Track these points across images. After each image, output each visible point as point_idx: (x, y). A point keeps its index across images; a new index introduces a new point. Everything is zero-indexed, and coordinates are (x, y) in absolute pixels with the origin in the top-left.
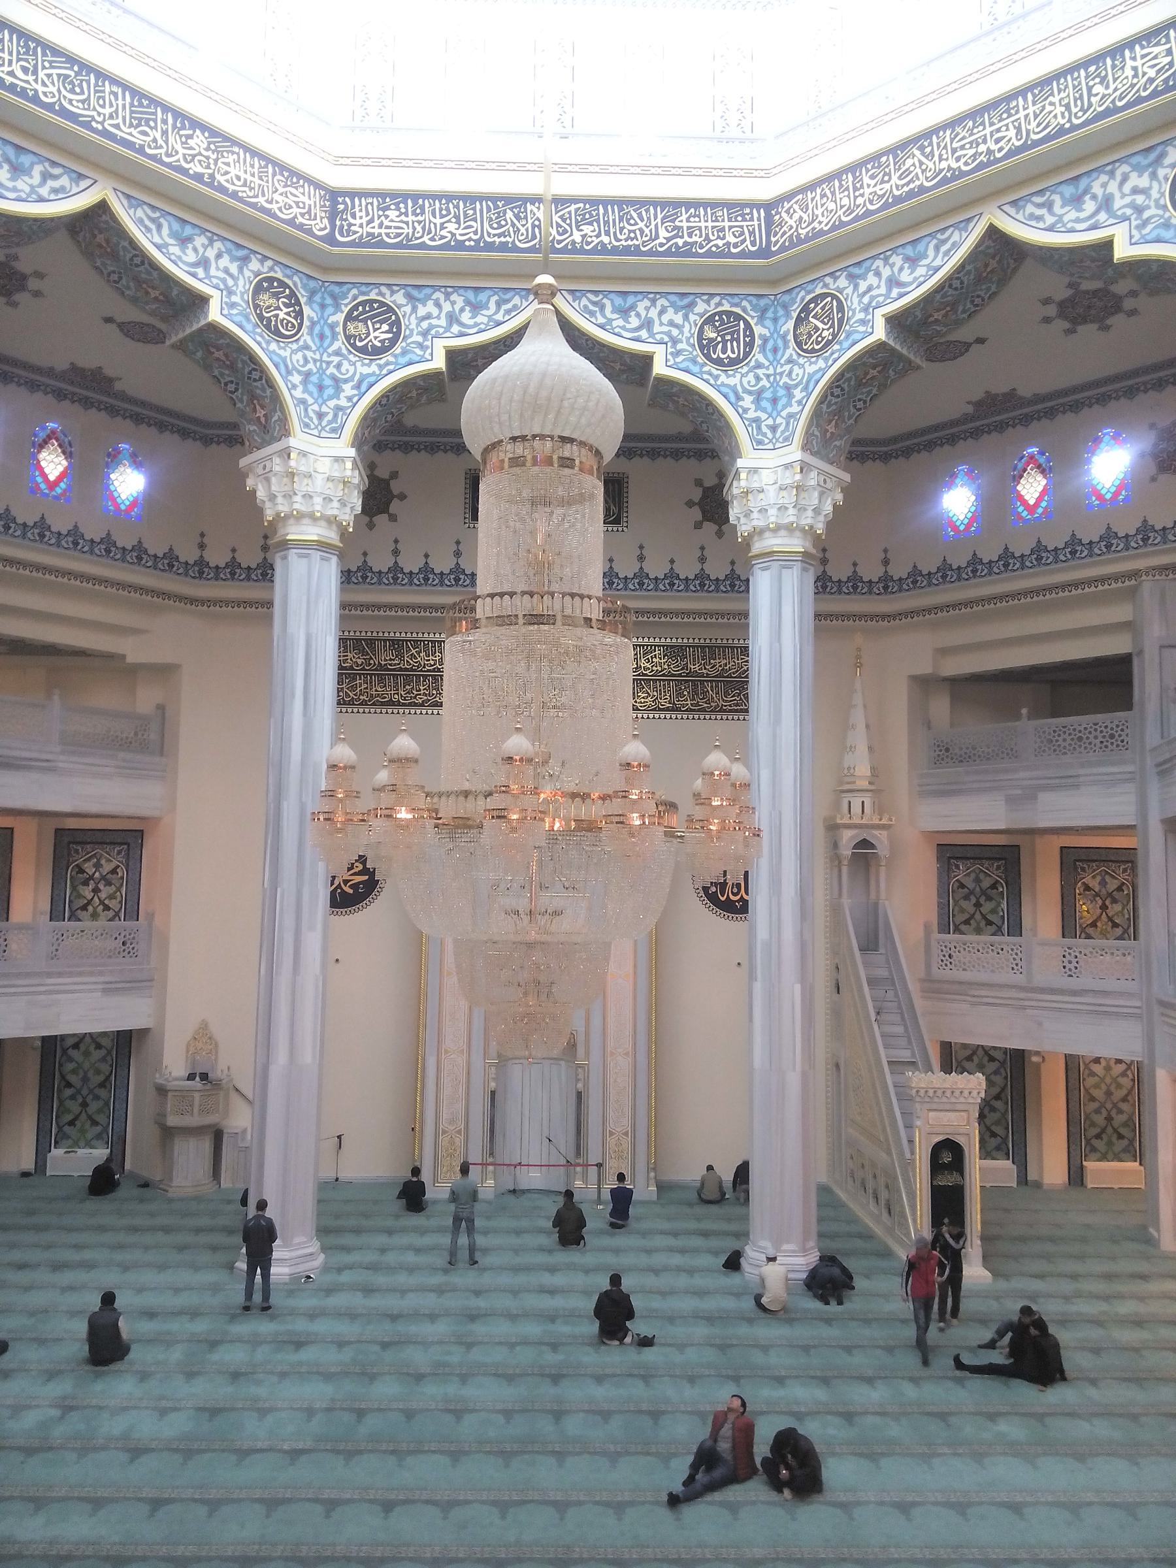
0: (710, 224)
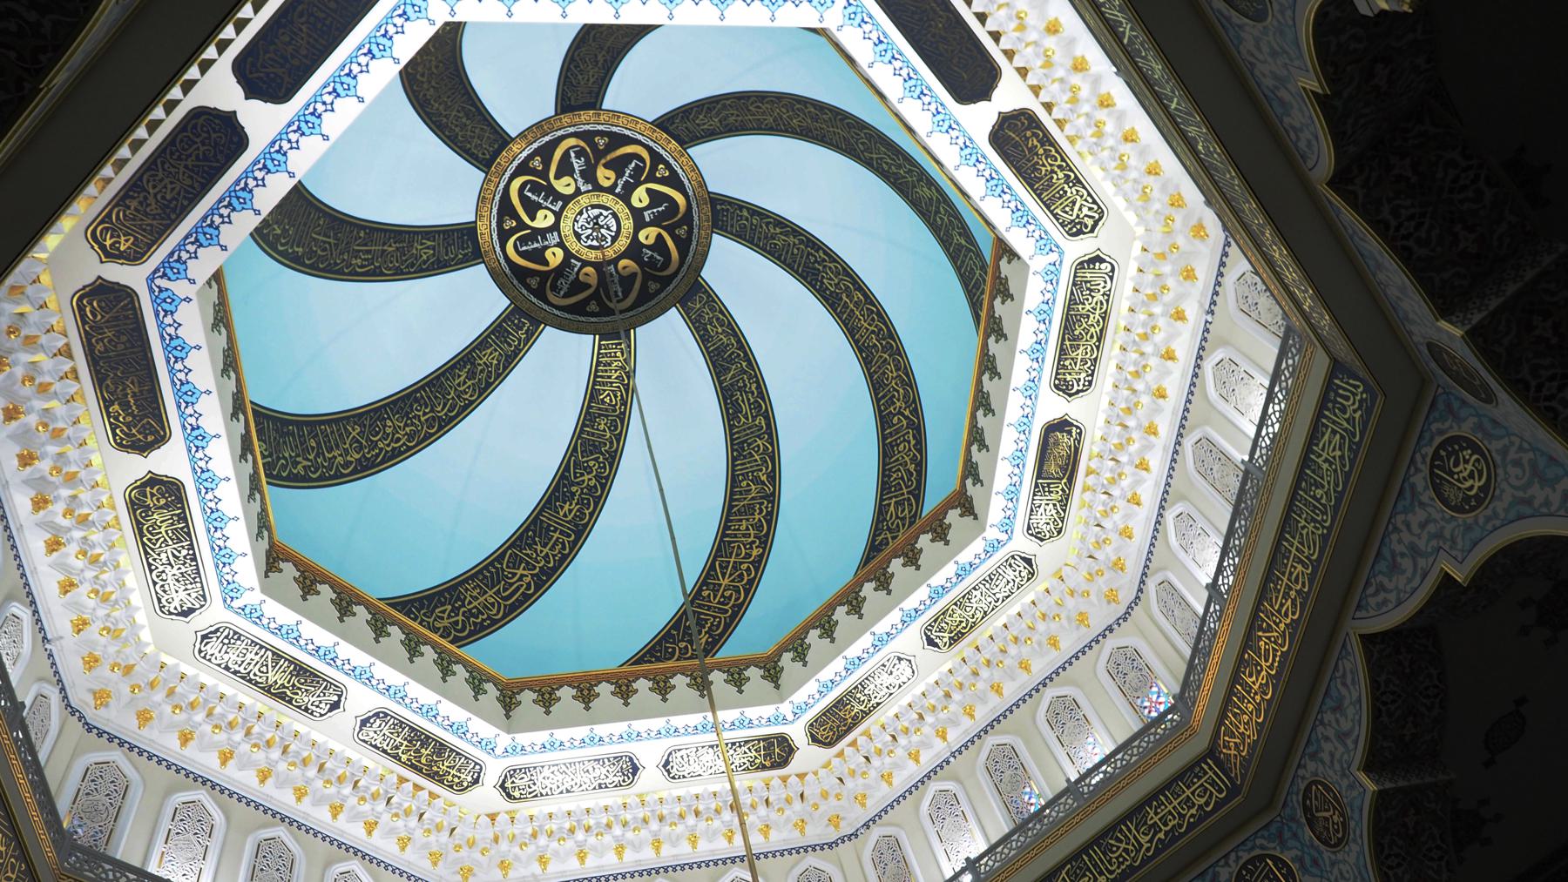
0: (1175, 803)
